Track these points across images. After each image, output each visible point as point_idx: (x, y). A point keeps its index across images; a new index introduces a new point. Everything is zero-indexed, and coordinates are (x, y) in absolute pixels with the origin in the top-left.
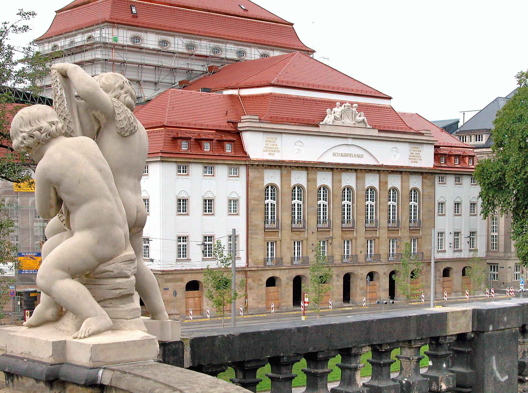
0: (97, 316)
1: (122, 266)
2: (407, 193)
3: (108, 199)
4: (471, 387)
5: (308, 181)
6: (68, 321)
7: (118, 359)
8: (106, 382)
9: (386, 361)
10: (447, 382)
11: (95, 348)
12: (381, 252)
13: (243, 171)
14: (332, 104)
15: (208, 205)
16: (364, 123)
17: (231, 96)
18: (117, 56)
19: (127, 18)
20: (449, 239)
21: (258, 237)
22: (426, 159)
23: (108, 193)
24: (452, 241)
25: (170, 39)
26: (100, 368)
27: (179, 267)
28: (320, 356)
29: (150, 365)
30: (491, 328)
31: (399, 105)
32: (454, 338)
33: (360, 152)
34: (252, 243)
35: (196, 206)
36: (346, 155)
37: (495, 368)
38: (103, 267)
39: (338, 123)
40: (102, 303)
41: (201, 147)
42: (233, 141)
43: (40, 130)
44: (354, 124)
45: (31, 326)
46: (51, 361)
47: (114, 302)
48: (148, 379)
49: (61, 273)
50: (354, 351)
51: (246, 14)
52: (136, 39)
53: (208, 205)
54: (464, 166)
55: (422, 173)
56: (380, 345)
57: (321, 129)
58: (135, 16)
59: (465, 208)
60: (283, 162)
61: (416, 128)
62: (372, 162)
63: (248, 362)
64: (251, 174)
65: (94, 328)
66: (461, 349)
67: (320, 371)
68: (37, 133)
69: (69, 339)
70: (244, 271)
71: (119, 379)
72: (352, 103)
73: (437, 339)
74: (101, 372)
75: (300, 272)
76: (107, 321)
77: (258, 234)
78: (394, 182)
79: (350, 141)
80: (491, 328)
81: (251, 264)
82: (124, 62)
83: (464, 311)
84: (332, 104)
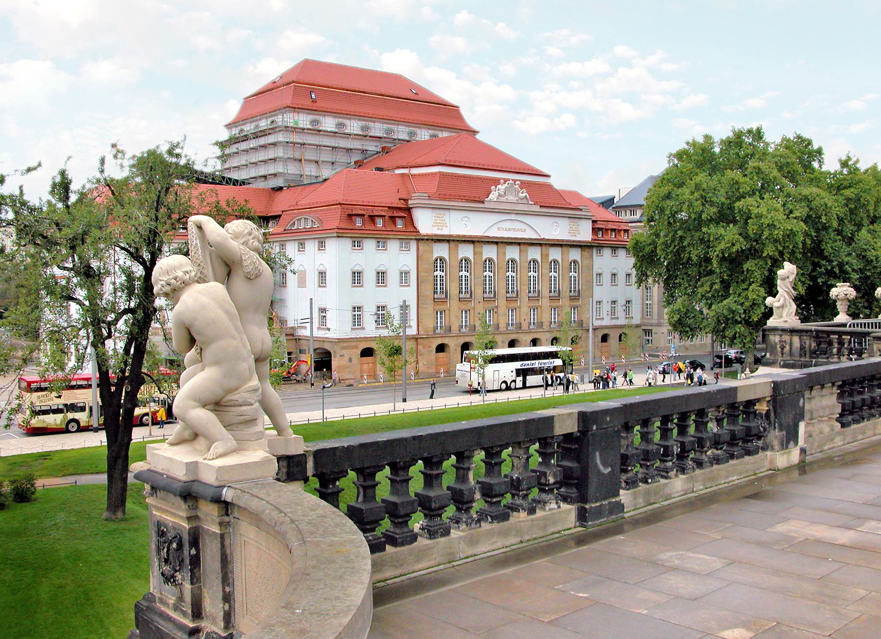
0: (225, 439)
1: (246, 395)
2: (567, 265)
3: (233, 338)
4: (577, 479)
5: (474, 254)
6: (201, 443)
7: (241, 478)
8: (229, 500)
9: (497, 460)
10: (555, 476)
11: (221, 469)
12: (544, 320)
13: (413, 245)
14: (496, 182)
15: (381, 277)
17: (402, 174)
18: (298, 138)
19: (308, 103)
20: (606, 307)
22: (585, 234)
23: (234, 333)
24: (610, 310)
25: (347, 122)
26: (224, 486)
28: (435, 460)
29: (268, 484)
30: (595, 428)
31: (558, 182)
32: (562, 438)
33: (523, 226)
35: (369, 278)
36: (510, 230)
37: (598, 461)
38: (230, 397)
39: (502, 199)
40: (229, 428)
41: (374, 222)
42: (404, 217)
43: (175, 279)
45: (172, 444)
46: (184, 478)
47: (239, 426)
48: (262, 499)
49: (192, 403)
50: (466, 454)
51: (416, 98)
52: (315, 122)
53: (381, 277)
54: (620, 239)
55: (580, 246)
56: (492, 448)
57: (486, 205)
58: (314, 101)
59: (621, 278)
60: (451, 236)
61: (574, 204)
62: (534, 236)
63: (367, 468)
64: (420, 248)
65: (220, 450)
66: (569, 446)
67: (435, 472)
68: (173, 281)
69: (200, 459)
70: (416, 339)
71: (239, 497)
72: (515, 181)
73: (545, 439)
74: (225, 490)
75: (467, 340)
76: (233, 443)
77: (427, 304)
78: (555, 254)
79: (513, 217)
80: (595, 428)
82: (304, 144)
83: (570, 414)
84: (496, 182)
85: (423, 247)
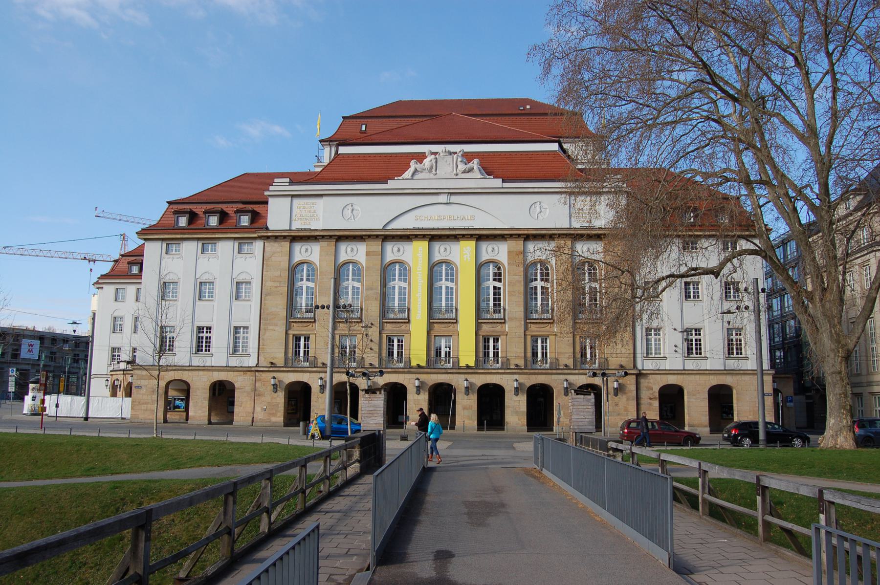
34: (267, 335)
57: (392, 184)
79: (443, 198)
81: (263, 362)
85: (272, 246)
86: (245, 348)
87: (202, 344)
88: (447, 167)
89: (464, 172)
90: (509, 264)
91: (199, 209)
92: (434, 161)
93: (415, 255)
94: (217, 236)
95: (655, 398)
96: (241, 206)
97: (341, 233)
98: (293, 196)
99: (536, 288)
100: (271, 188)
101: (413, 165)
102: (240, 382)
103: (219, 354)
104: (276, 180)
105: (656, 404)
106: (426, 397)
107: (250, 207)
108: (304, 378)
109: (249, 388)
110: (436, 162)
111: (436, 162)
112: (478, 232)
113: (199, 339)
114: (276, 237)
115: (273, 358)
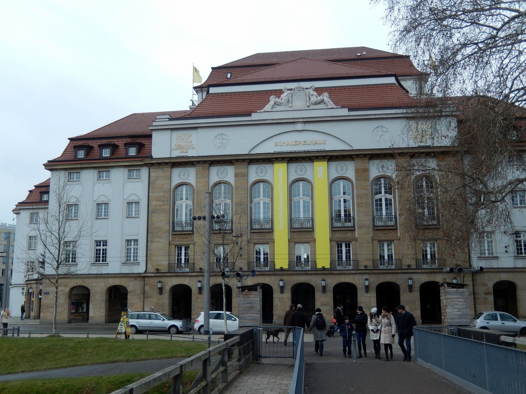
5: (236, 175)
15: (102, 209)
16: (325, 103)
21: (161, 240)
27: (95, 270)
33: (320, 138)
34: (153, 246)
39: (278, 108)
44: (308, 106)
57: (255, 116)
64: (152, 174)
77: (161, 237)
79: (299, 127)
85: (156, 173)
86: (136, 256)
87: (101, 256)
88: (299, 102)
89: (316, 103)
90: (356, 180)
91: (95, 144)
92: (290, 95)
93: (279, 174)
94: (110, 165)
95: (490, 293)
96: (129, 140)
97: (214, 159)
98: (172, 129)
99: (381, 200)
100: (154, 124)
101: (273, 99)
102: (131, 286)
103: (115, 265)
104: (158, 117)
105: (491, 298)
106: (290, 295)
107: (139, 140)
108: (186, 281)
109: (139, 291)
110: (292, 96)
111: (292, 96)
112: (329, 154)
113: (98, 251)
114: (159, 164)
115: (159, 266)
